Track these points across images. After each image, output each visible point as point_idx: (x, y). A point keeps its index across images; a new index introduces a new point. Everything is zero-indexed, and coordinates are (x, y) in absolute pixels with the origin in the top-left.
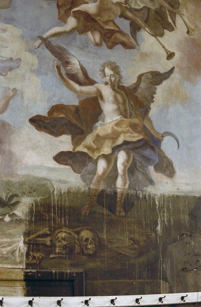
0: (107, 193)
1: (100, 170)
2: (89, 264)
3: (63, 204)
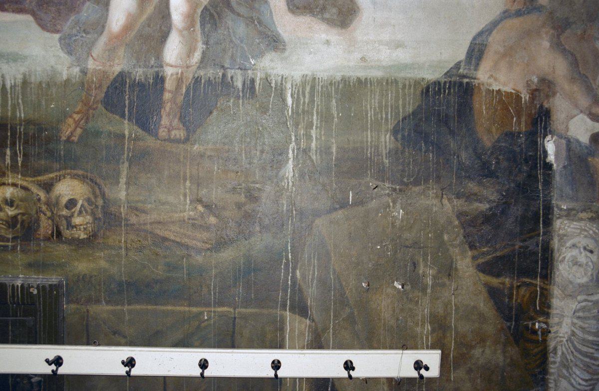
0: (135, 79)
1: (118, 20)
2: (76, 264)
3: (9, 114)
